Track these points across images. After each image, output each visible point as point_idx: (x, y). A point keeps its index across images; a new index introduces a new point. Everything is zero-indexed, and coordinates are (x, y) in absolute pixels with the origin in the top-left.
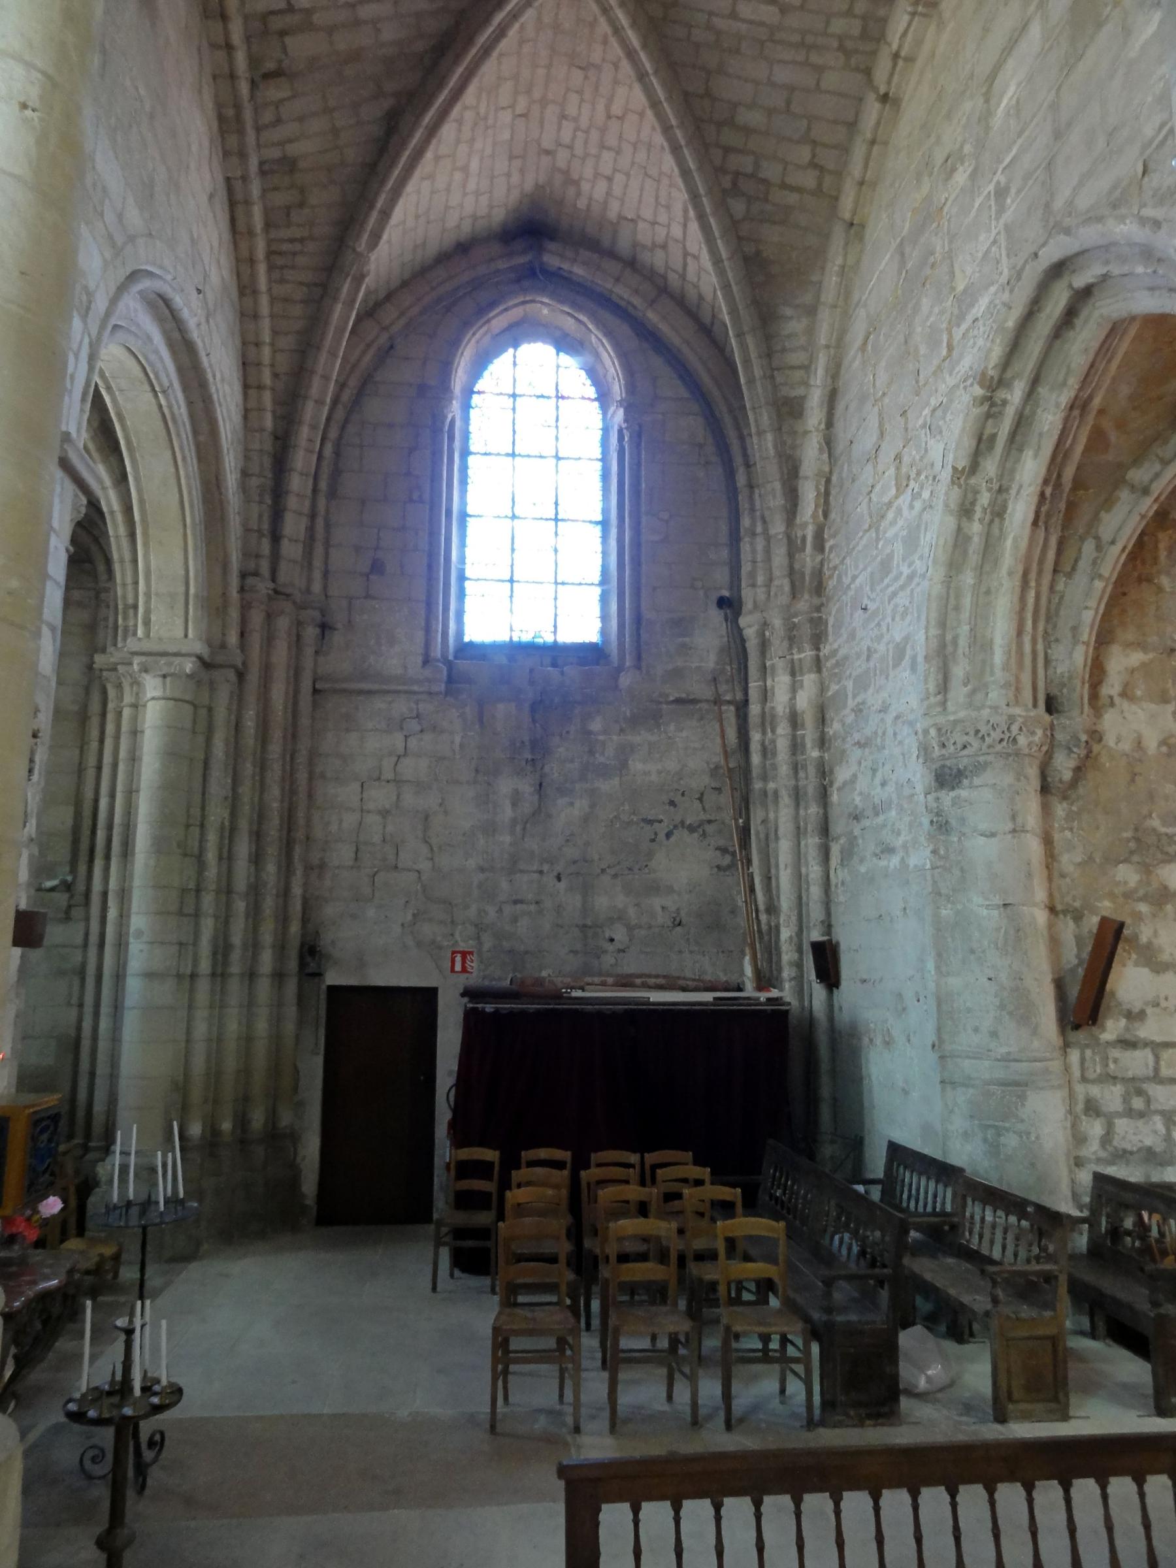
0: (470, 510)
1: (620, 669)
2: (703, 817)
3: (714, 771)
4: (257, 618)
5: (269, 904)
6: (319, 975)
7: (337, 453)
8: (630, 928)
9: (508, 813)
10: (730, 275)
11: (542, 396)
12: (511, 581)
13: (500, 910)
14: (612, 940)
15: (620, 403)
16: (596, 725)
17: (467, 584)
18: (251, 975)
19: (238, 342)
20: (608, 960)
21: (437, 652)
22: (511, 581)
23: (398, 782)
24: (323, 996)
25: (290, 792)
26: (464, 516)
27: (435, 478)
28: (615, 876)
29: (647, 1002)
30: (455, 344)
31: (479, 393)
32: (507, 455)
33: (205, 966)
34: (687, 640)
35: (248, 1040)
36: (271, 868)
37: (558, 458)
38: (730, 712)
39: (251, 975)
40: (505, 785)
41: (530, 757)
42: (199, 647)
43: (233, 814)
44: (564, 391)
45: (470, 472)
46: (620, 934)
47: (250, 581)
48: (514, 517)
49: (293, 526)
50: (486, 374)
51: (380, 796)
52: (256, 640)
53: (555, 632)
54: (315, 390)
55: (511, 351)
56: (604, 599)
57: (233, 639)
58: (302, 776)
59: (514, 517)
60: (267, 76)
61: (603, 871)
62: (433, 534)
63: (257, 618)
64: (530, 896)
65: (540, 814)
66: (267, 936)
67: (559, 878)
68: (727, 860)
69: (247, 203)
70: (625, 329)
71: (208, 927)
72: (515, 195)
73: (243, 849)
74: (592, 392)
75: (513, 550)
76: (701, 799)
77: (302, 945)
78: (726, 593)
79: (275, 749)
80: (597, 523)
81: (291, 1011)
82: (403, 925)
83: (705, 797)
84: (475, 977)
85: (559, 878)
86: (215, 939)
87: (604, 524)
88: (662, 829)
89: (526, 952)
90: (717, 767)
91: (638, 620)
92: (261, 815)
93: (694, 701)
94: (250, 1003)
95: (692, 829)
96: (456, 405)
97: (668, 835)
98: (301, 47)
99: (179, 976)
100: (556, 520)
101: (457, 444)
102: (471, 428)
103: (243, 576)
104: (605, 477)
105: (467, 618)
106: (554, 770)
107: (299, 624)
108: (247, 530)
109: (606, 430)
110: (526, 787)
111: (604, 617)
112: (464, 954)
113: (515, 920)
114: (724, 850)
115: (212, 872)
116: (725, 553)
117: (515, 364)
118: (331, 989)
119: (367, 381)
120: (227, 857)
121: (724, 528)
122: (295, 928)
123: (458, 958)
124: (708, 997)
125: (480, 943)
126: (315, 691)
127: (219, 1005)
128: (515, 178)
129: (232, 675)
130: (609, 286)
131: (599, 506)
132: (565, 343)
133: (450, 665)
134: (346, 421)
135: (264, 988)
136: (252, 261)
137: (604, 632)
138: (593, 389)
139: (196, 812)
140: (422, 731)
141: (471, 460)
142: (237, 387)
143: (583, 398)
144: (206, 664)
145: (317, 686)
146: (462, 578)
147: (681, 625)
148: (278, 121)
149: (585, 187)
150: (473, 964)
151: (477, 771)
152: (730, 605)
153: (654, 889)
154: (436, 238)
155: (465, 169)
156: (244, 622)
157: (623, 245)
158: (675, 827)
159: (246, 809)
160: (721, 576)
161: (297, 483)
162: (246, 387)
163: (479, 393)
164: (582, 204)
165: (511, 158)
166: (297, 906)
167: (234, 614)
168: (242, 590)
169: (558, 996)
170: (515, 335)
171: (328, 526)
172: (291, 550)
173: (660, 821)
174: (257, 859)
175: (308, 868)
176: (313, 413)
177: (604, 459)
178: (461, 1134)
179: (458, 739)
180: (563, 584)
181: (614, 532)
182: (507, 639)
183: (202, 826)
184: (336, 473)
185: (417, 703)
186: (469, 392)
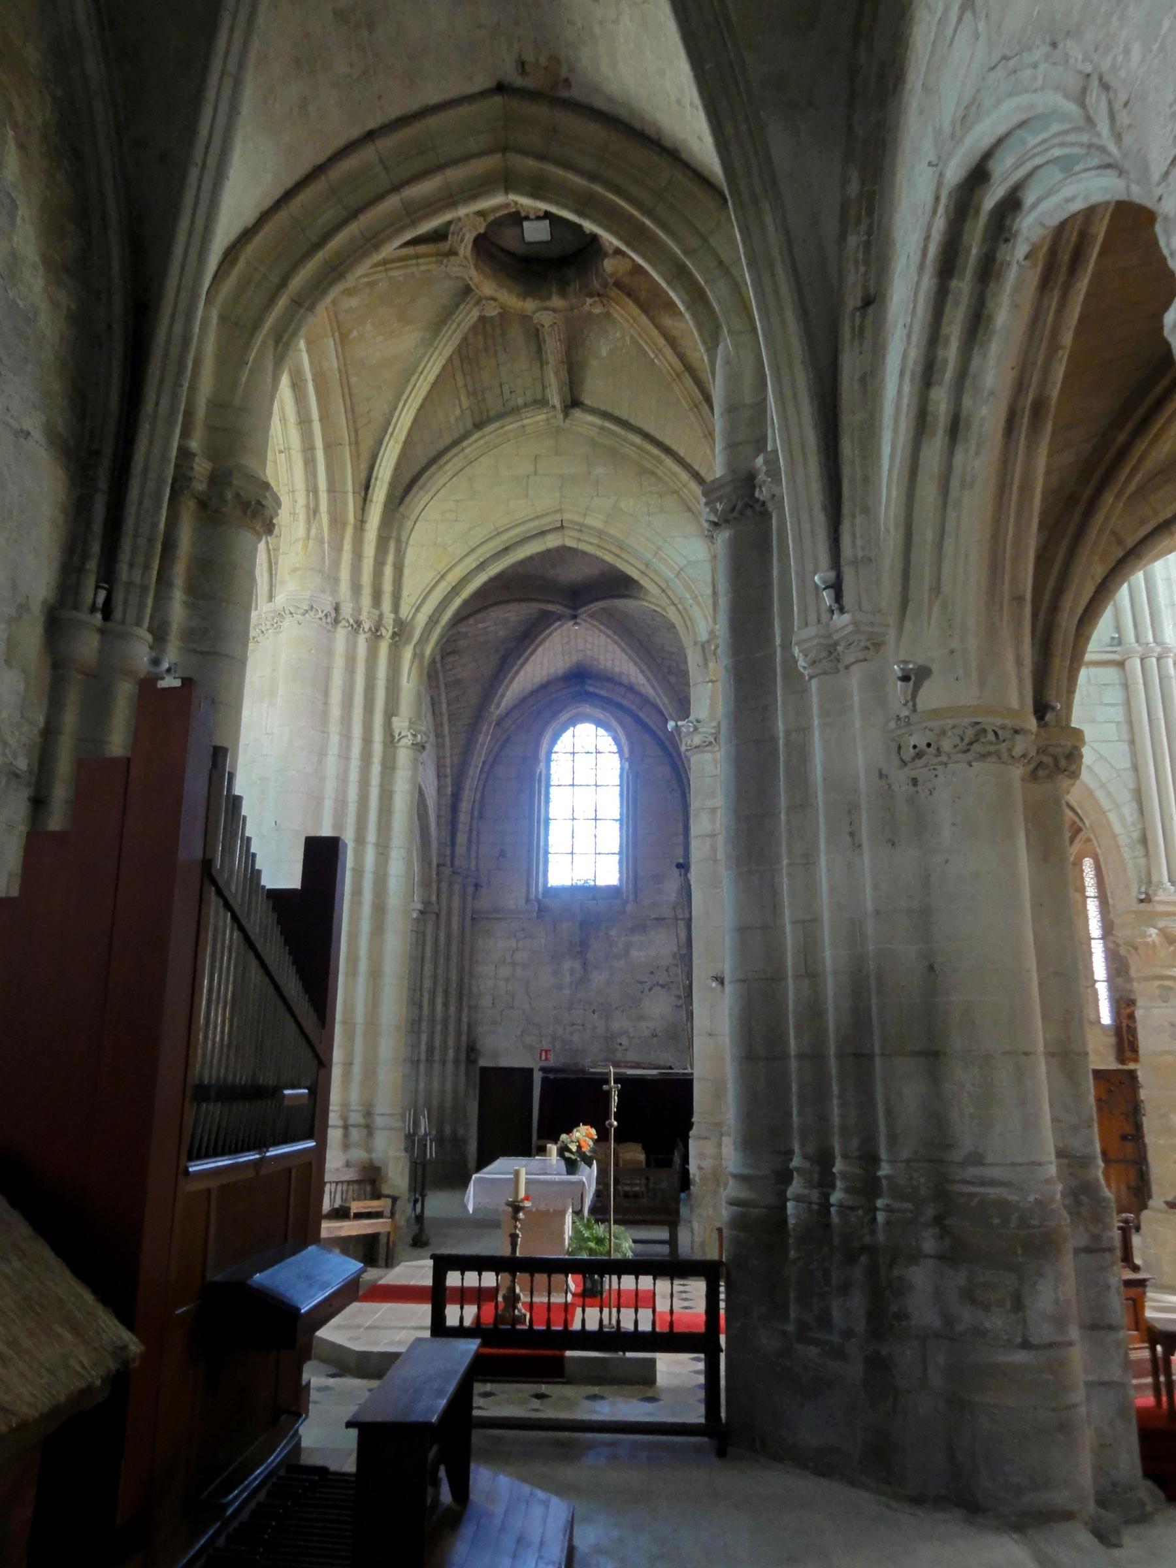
0: (551, 816)
1: (627, 902)
2: (668, 979)
3: (674, 955)
4: (444, 886)
5: (452, 1026)
6: (475, 1061)
7: (483, 796)
8: (630, 1038)
9: (567, 979)
10: (671, 710)
11: (588, 753)
12: (572, 853)
13: (565, 1029)
14: (621, 1044)
15: (627, 760)
16: (613, 933)
17: (549, 856)
18: (444, 1062)
19: (436, 760)
20: (619, 1055)
21: (533, 896)
22: (572, 853)
23: (514, 964)
24: (478, 1072)
25: (461, 970)
26: (547, 820)
27: (532, 806)
28: (623, 1011)
29: (625, 1074)
30: (541, 734)
31: (556, 752)
32: (570, 785)
33: (423, 1057)
34: (661, 885)
35: (442, 1092)
36: (452, 1009)
37: (596, 785)
38: (681, 924)
39: (444, 1062)
40: (567, 965)
41: (579, 949)
42: (420, 906)
43: (435, 984)
44: (600, 749)
45: (551, 796)
46: (625, 1041)
47: (441, 868)
48: (574, 819)
49: (461, 839)
50: (559, 742)
51: (505, 971)
52: (444, 897)
53: (595, 881)
54: (471, 773)
55: (572, 729)
56: (620, 862)
57: (434, 898)
58: (466, 963)
59: (574, 819)
60: (448, 654)
61: (616, 1008)
62: (531, 834)
63: (444, 886)
64: (579, 1022)
65: (584, 980)
66: (451, 1042)
67: (594, 1012)
68: (680, 1003)
69: (440, 703)
70: (628, 720)
71: (424, 1038)
72: (568, 665)
73: (439, 1000)
74: (614, 748)
75: (573, 837)
76: (667, 971)
77: (467, 1047)
78: (681, 861)
79: (454, 949)
80: (617, 820)
81: (462, 1079)
82: (516, 1036)
83: (670, 970)
84: (551, 1063)
85: (594, 1012)
86: (427, 1044)
87: (621, 820)
88: (647, 987)
89: (577, 1050)
90: (675, 954)
91: (636, 877)
92: (448, 980)
93: (664, 919)
94: (443, 1076)
95: (662, 986)
96: (542, 765)
97: (650, 990)
98: (462, 644)
99: (412, 1061)
100: (596, 819)
101: (543, 784)
102: (551, 772)
103: (439, 866)
104: (621, 795)
105: (550, 875)
106: (591, 956)
107: (464, 886)
108: (440, 844)
109: (622, 769)
110: (577, 965)
111: (621, 872)
112: (546, 1051)
113: (571, 1034)
114: (679, 997)
115: (426, 1011)
116: (681, 838)
117: (574, 736)
118: (484, 1070)
119: (497, 755)
120: (433, 1004)
121: (681, 825)
122: (464, 1038)
123: (544, 1054)
124: (655, 1072)
125: (554, 1046)
126: (473, 919)
127: (429, 1074)
128: (568, 660)
129: (434, 916)
130: (619, 700)
131: (618, 811)
132: (599, 723)
133: (537, 900)
134: (487, 778)
135: (450, 1067)
136: (442, 724)
137: (620, 879)
138: (615, 747)
139: (418, 983)
140: (525, 937)
141: (552, 790)
142: (436, 783)
143: (610, 752)
144: (421, 912)
145: (474, 916)
146: (547, 853)
147: (658, 878)
148: (454, 668)
149: (602, 662)
150: (551, 1056)
151: (553, 958)
152: (684, 867)
153: (642, 1018)
154: (529, 687)
155: (542, 664)
156: (439, 888)
157: (625, 681)
158: (654, 985)
159: (441, 980)
160: (679, 851)
161: (463, 818)
162: (439, 776)
163: (556, 752)
164: (602, 667)
165: (563, 655)
166: (464, 1027)
167: (434, 886)
168: (438, 874)
169: (583, 1071)
170: (573, 722)
171: (478, 835)
172: (460, 850)
173: (646, 982)
174: (446, 1005)
175: (470, 1008)
176: (470, 784)
177: (621, 785)
178: (539, 1138)
179: (543, 940)
180: (599, 854)
181: (625, 827)
182: (570, 884)
183: (421, 990)
184: (482, 805)
185: (523, 923)
186: (549, 752)
